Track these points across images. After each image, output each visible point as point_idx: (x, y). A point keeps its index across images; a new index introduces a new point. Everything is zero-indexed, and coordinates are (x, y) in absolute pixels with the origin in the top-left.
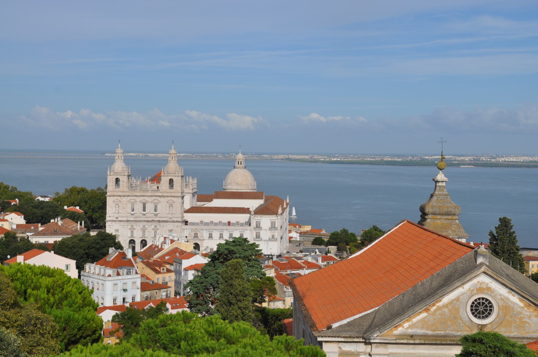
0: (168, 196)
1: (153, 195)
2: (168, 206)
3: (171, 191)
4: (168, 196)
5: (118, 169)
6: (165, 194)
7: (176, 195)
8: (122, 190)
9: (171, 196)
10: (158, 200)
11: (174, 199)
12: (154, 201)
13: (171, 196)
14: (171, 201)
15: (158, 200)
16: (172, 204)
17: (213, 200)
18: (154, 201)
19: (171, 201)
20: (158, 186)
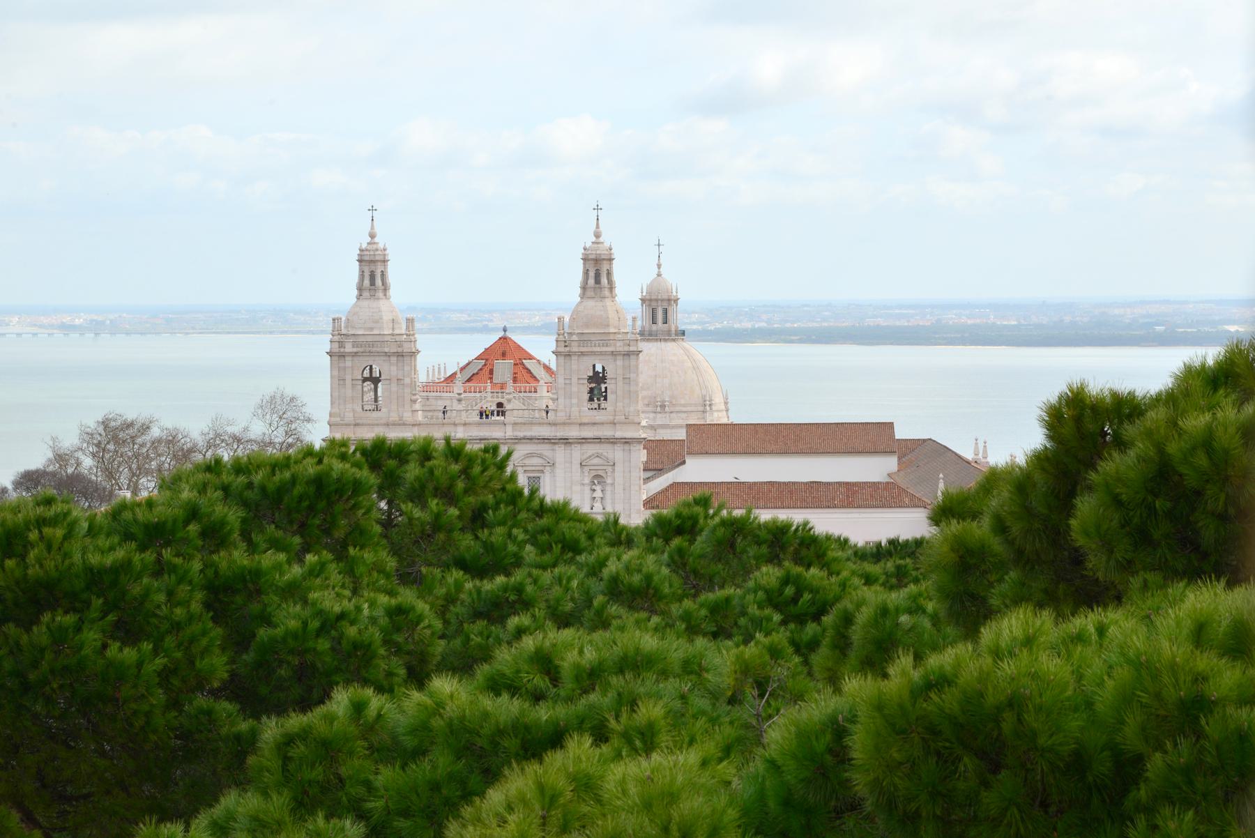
0: (583, 441)
1: (521, 434)
2: (587, 481)
3: (599, 416)
4: (583, 441)
5: (372, 329)
6: (573, 433)
7: (619, 434)
8: (394, 417)
9: (598, 440)
10: (540, 456)
11: (606, 450)
12: (527, 462)
13: (598, 440)
14: (596, 461)
15: (540, 456)
16: (600, 473)
17: (684, 463)
18: (527, 462)
19: (596, 461)
20: (500, 400)
